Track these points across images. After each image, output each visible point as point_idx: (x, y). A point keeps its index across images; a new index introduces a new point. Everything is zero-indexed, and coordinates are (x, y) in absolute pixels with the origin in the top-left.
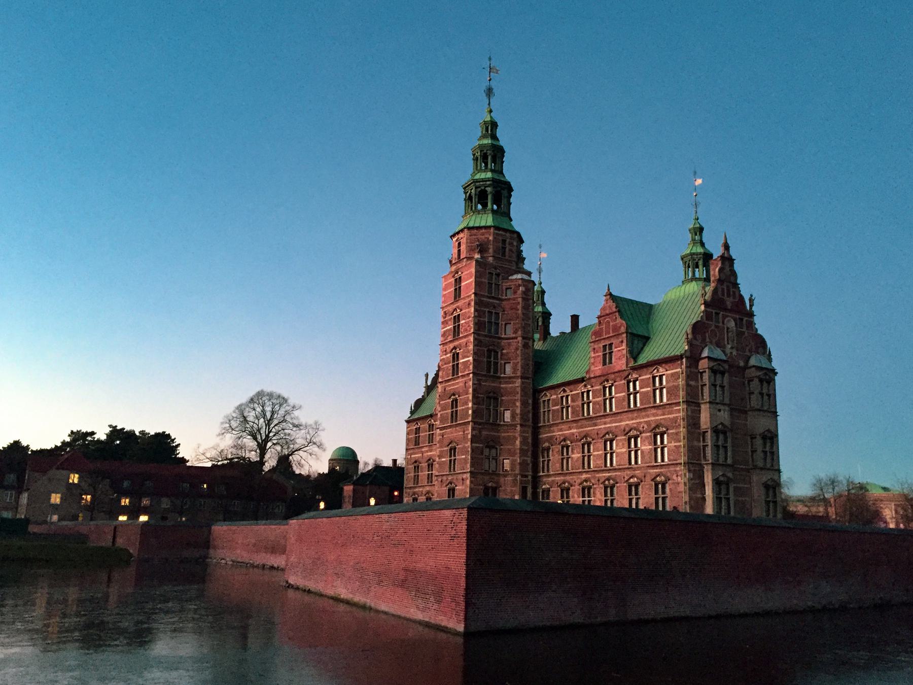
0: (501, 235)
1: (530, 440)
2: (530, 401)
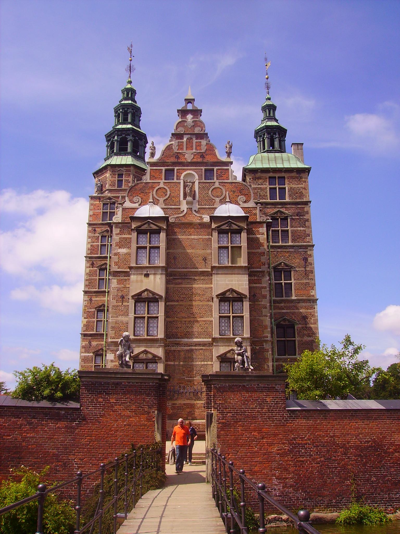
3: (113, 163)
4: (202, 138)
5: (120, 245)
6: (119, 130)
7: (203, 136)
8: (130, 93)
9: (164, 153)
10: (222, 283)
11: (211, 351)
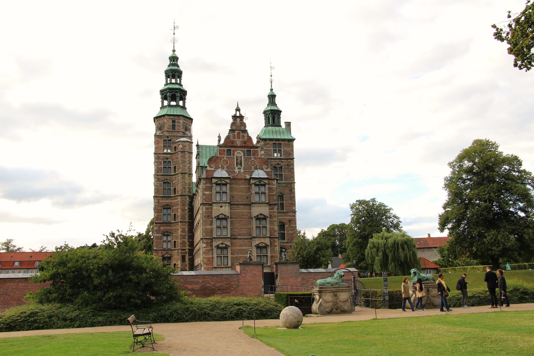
0: (172, 119)
1: (187, 229)
2: (186, 208)
3: (169, 113)
4: (245, 133)
7: (245, 131)
8: (174, 59)
9: (225, 140)
10: (256, 211)
11: (251, 242)
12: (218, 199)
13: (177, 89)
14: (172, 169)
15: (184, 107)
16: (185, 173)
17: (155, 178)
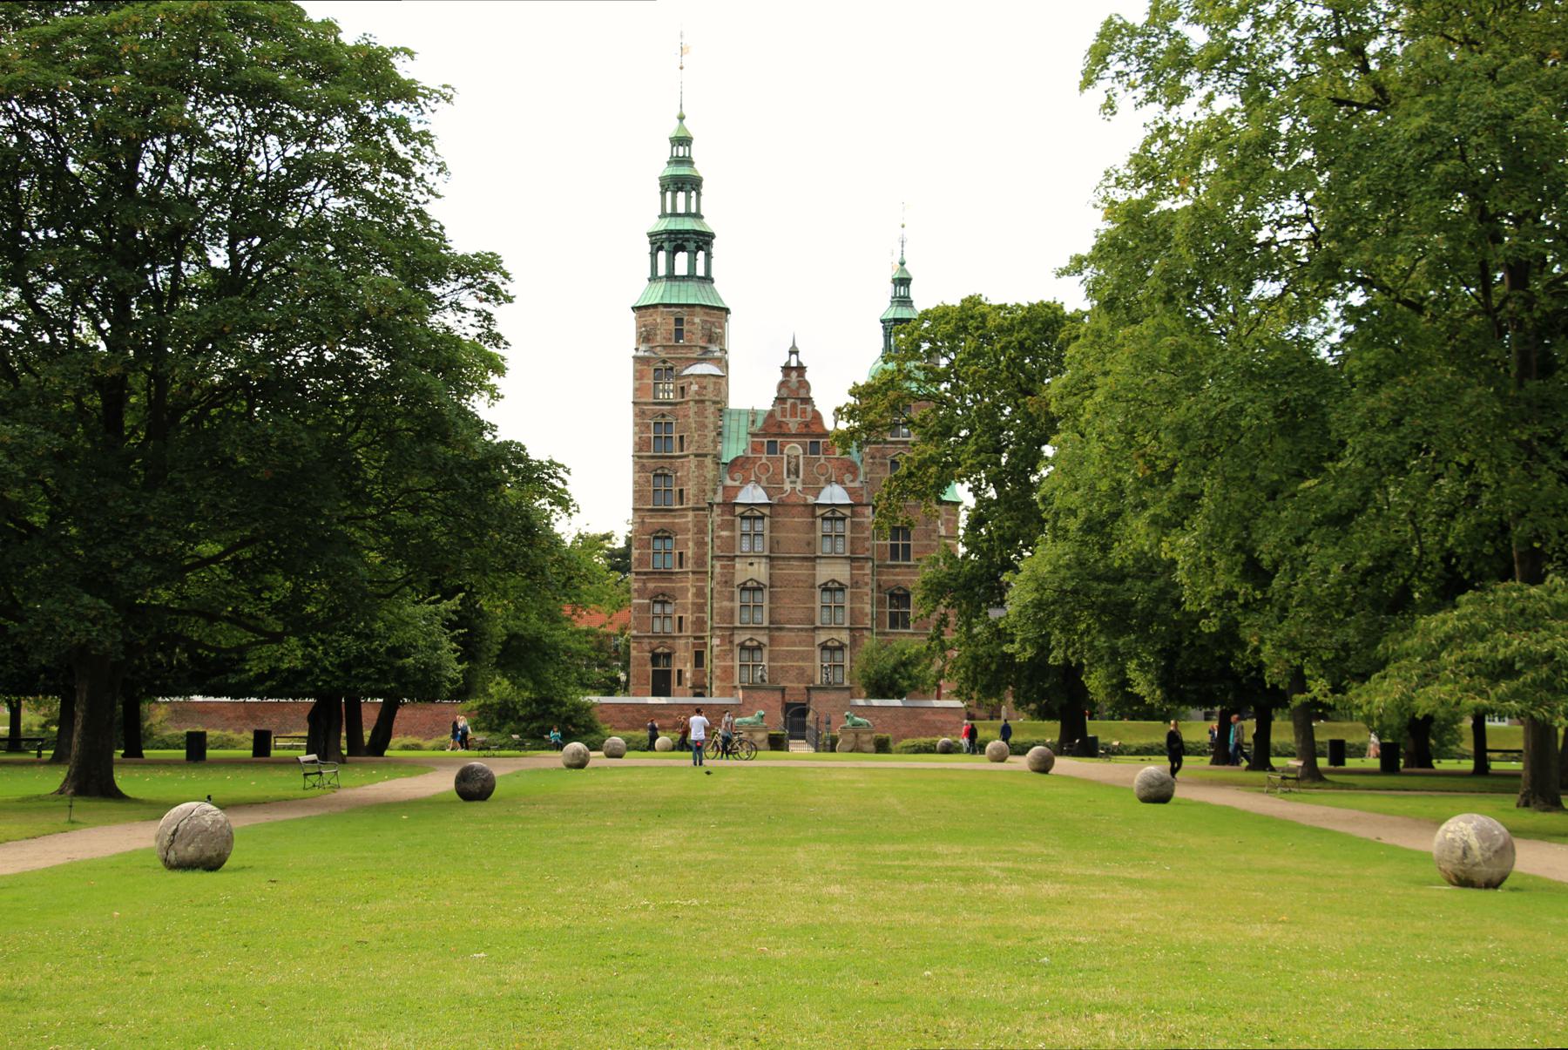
3: (666, 301)
5: (722, 526)
6: (670, 232)
7: (808, 401)
10: (827, 572)
12: (746, 547)
13: (687, 232)
14: (676, 442)
15: (708, 279)
16: (705, 455)
17: (635, 463)
